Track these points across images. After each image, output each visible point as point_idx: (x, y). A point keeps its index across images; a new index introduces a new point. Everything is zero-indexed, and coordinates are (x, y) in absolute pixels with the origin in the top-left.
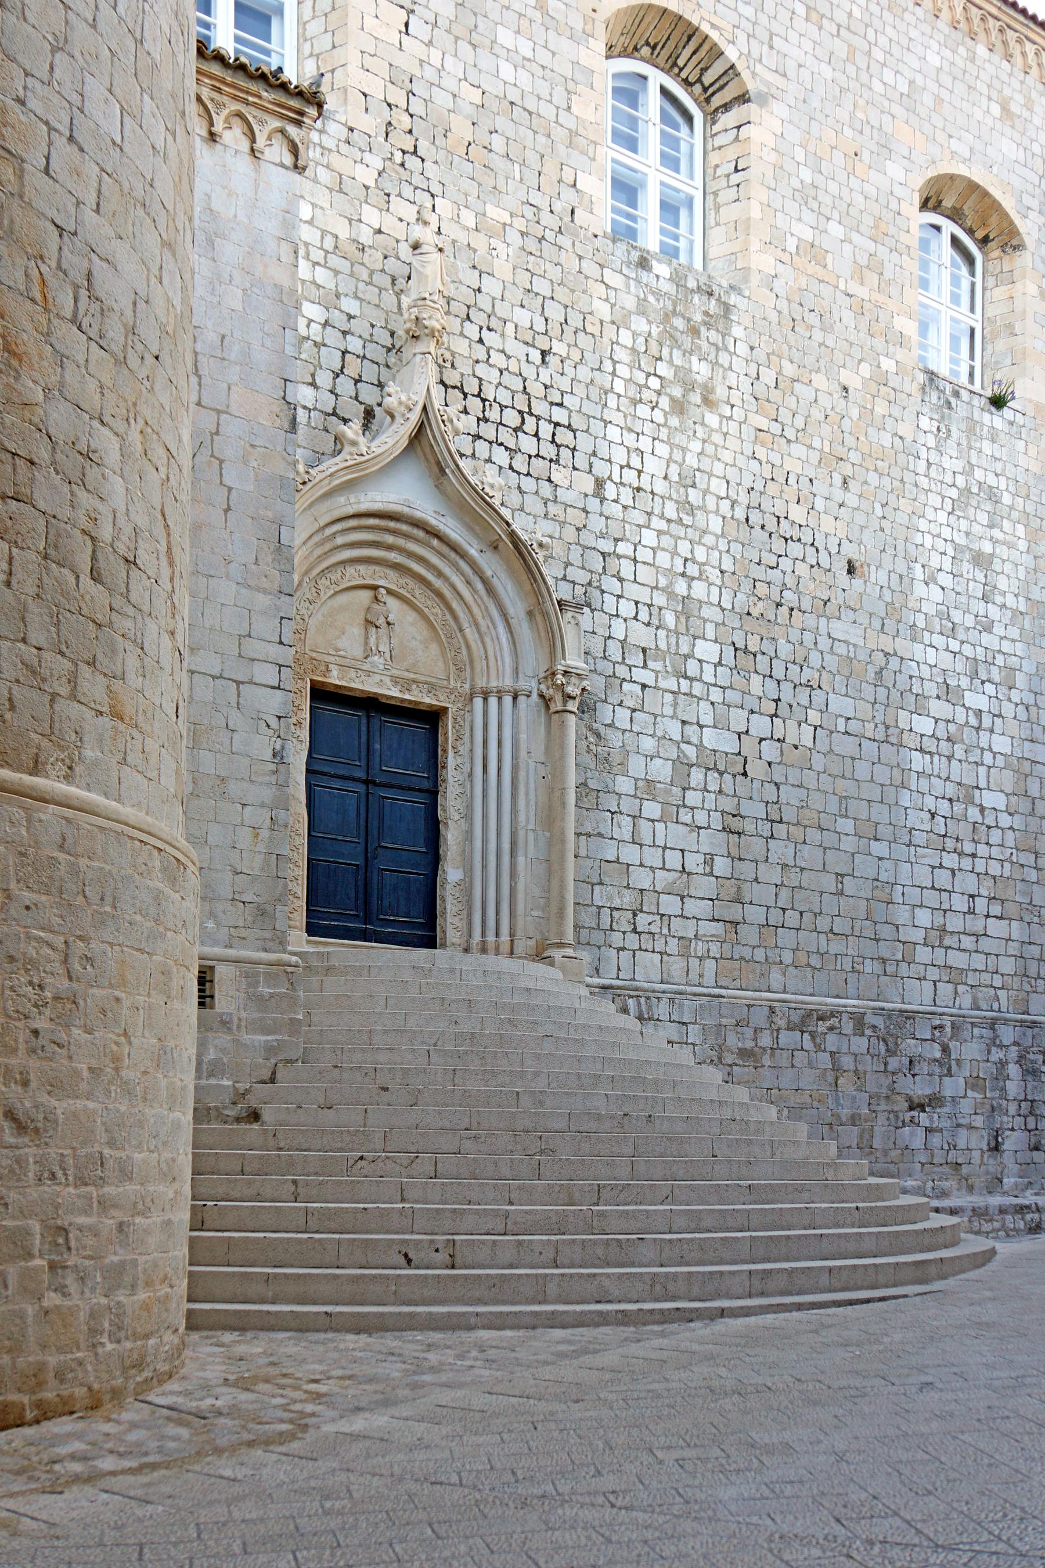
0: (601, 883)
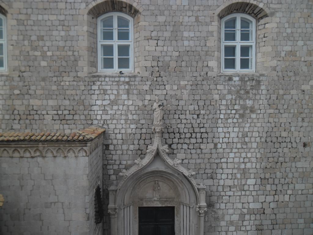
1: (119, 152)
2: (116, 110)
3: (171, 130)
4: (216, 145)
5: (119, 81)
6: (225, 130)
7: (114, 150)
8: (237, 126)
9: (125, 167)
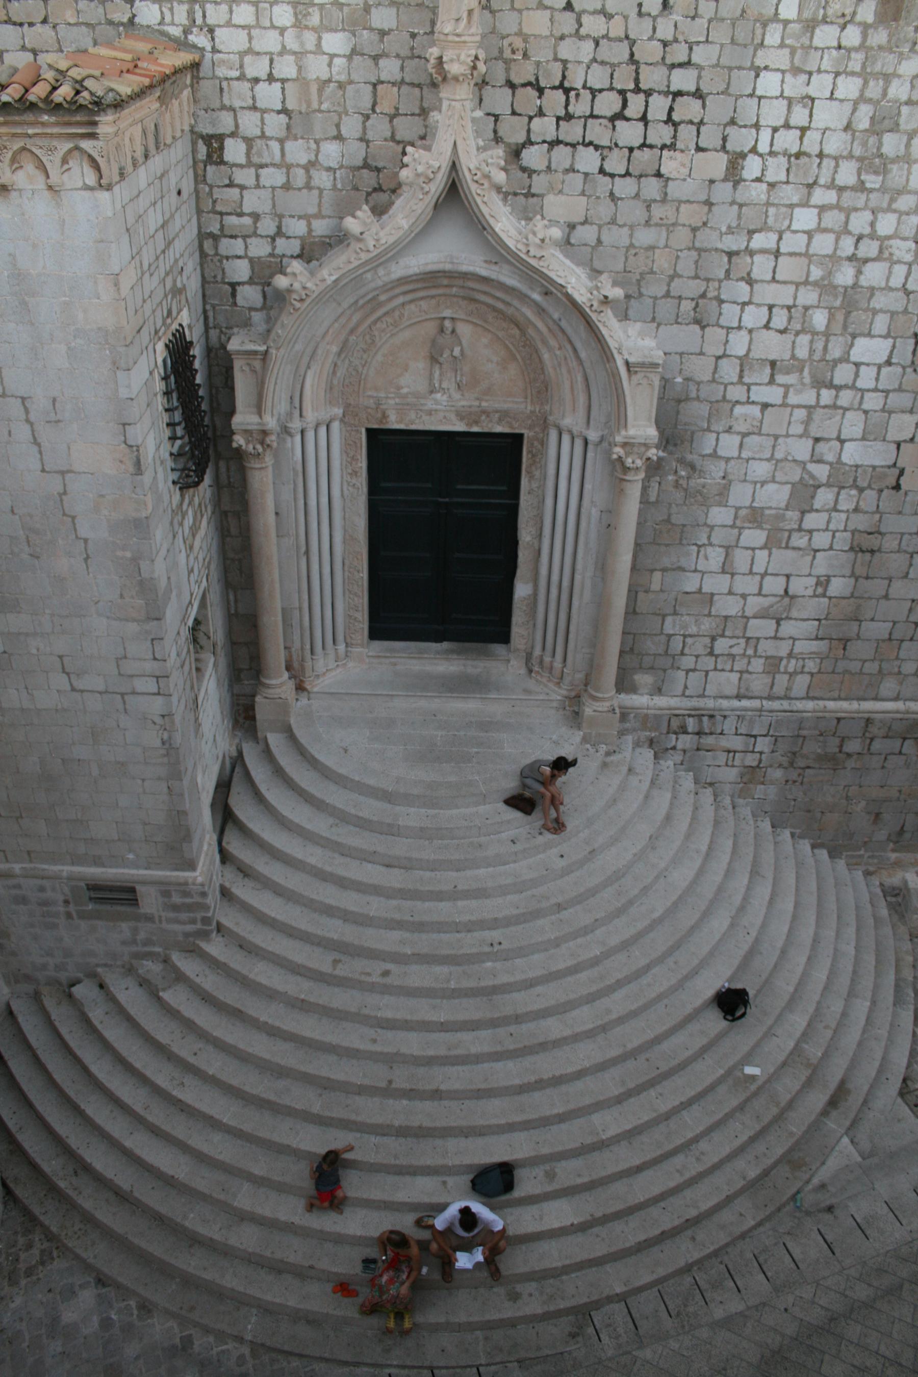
0: (675, 613)
1: (273, 177)
3: (523, 73)
4: (736, 161)
6: (795, 86)
8: (858, 69)
9: (303, 249)
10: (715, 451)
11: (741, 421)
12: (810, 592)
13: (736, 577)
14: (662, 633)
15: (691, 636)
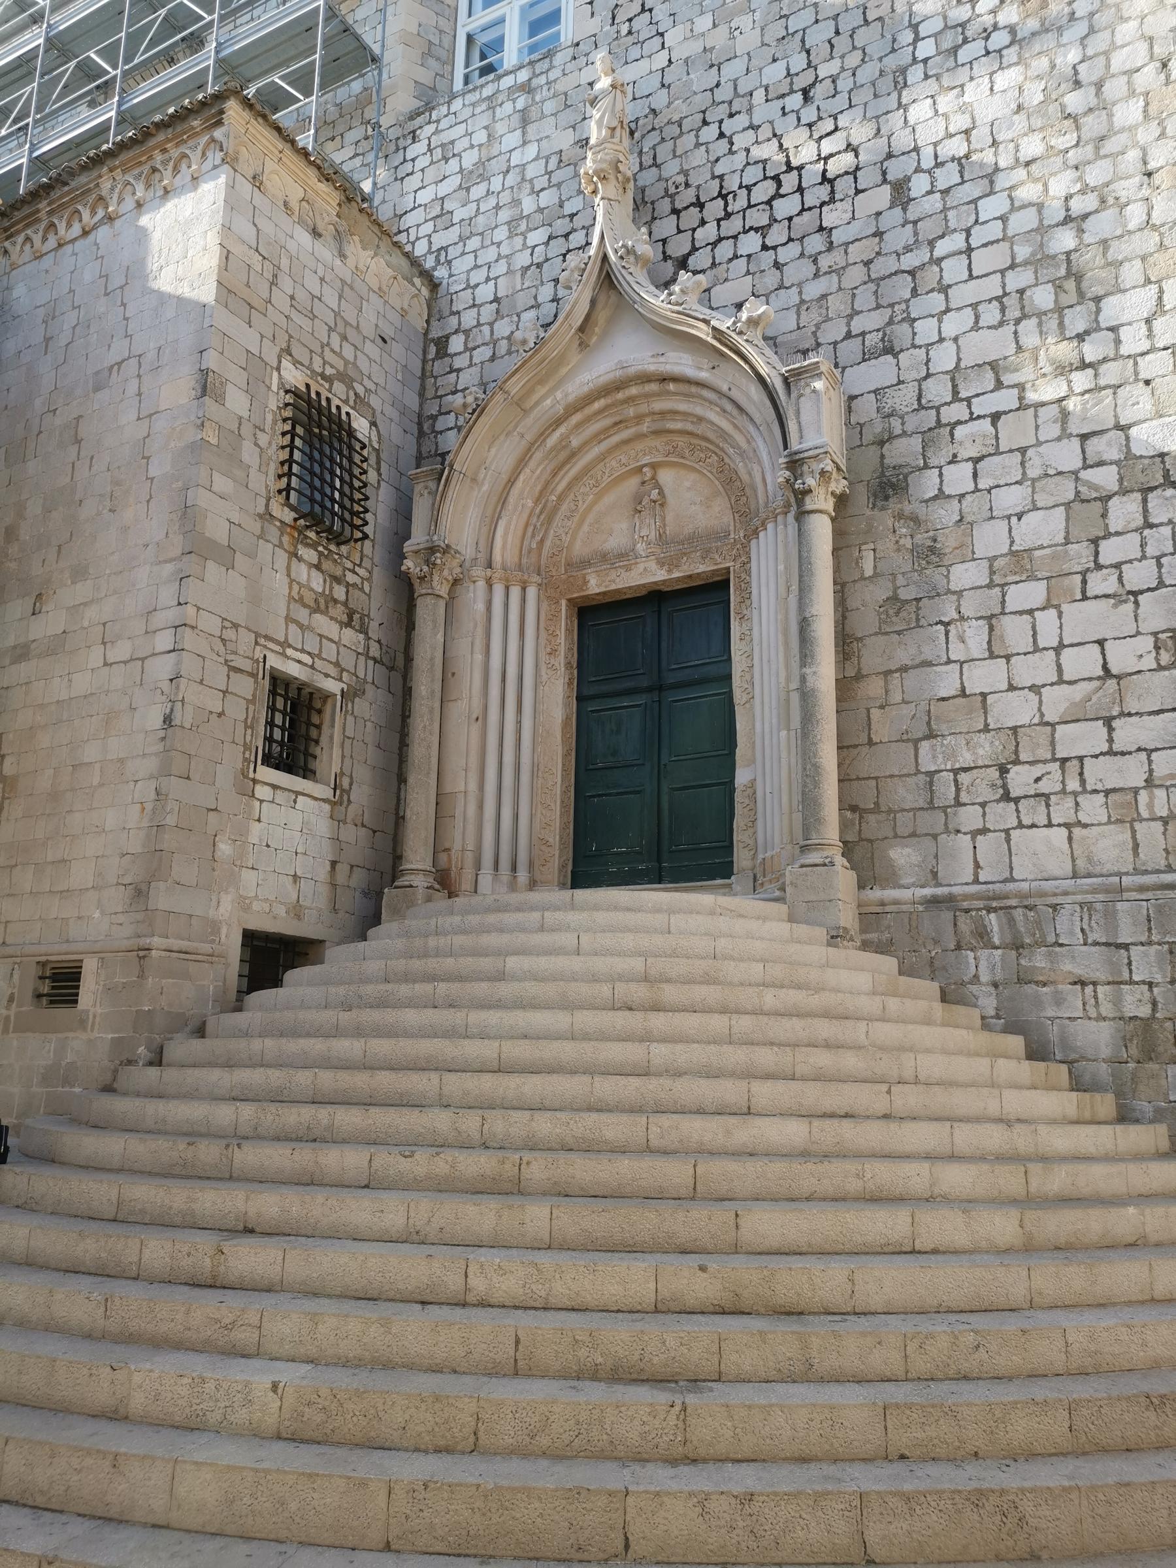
0: (931, 736)
2: (478, 201)
5: (498, 91)
7: (466, 349)
8: (1015, 59)
10: (940, 490)
11: (968, 444)
12: (1149, 662)
13: (1013, 660)
14: (918, 772)
15: (966, 770)
